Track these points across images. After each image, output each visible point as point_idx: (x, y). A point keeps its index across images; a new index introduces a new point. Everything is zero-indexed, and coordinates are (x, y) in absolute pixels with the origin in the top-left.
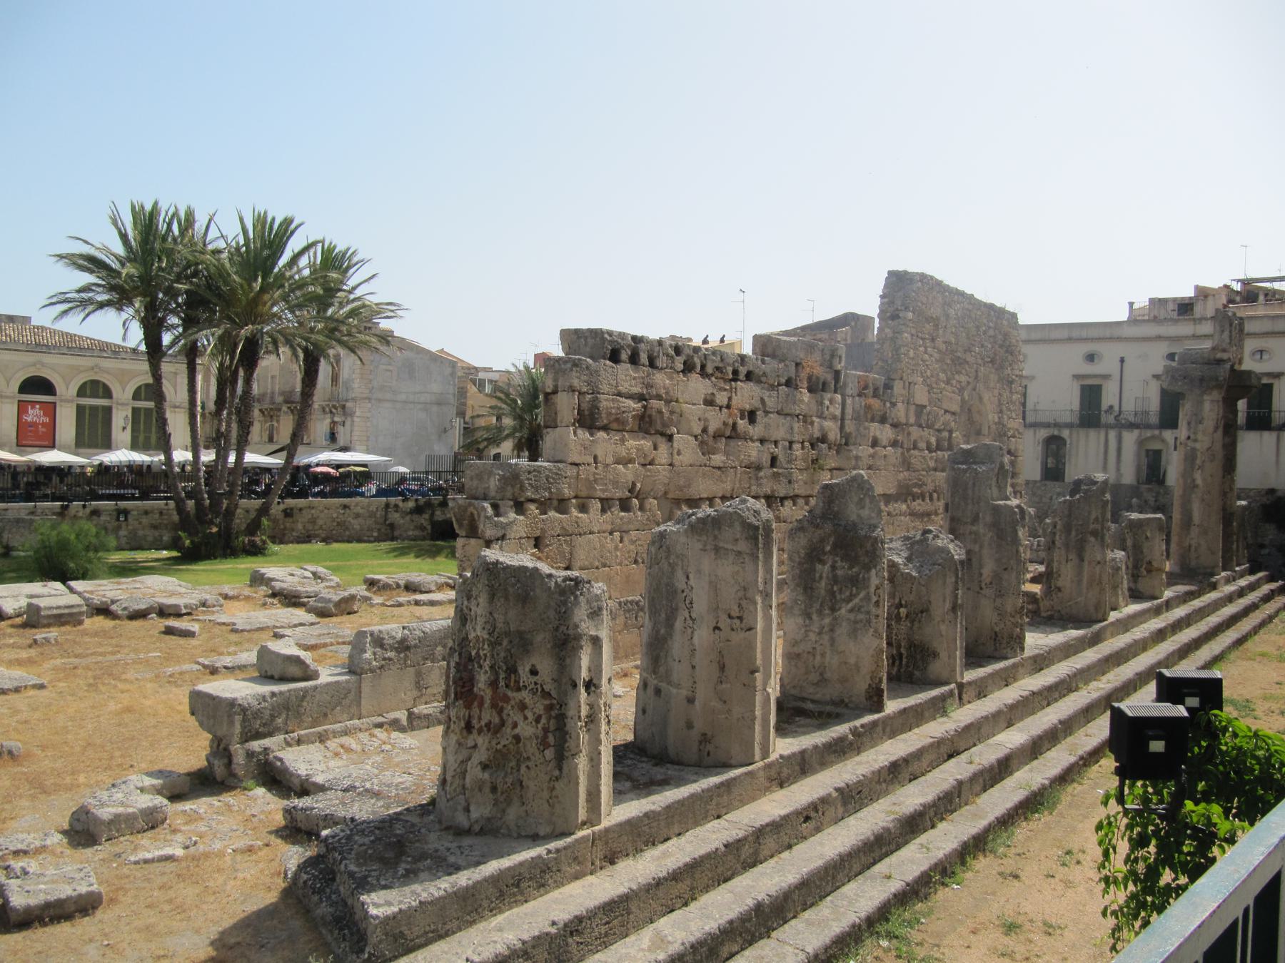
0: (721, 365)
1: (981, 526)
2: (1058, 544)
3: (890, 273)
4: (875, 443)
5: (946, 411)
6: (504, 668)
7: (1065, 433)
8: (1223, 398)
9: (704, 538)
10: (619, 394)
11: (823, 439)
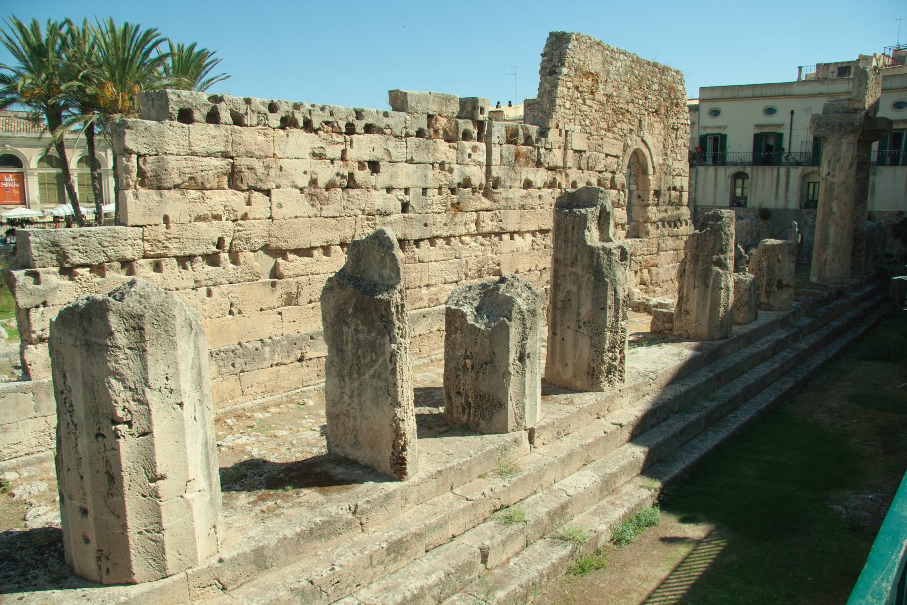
0: (331, 119)
1: (580, 268)
2: (687, 273)
3: (552, 34)
4: (528, 184)
5: (607, 155)
7: (748, 170)
8: (859, 140)
10: (194, 154)
11: (466, 183)
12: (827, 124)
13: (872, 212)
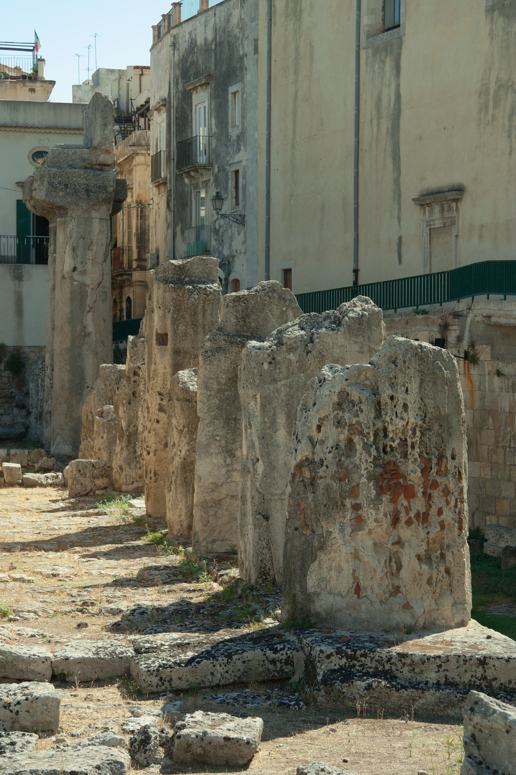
6: (437, 453)
9: (361, 339)
12: (66, 186)
13: (20, 348)
